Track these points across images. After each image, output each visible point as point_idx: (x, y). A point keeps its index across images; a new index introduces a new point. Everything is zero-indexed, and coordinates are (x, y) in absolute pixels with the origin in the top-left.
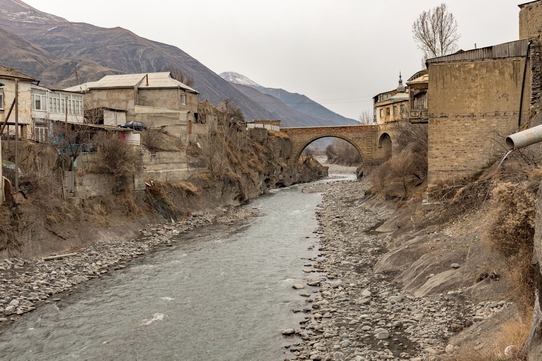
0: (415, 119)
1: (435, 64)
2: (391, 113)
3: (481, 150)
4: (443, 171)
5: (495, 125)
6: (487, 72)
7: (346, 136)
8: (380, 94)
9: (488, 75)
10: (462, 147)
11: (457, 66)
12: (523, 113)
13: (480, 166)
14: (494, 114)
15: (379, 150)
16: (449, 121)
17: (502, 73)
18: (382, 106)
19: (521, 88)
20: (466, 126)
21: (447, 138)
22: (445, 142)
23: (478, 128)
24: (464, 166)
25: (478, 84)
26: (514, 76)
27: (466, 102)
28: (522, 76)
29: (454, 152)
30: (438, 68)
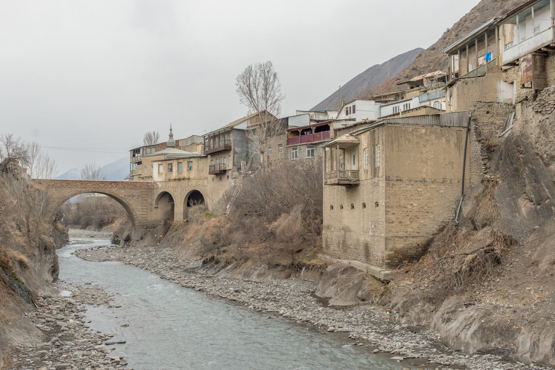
0: (344, 180)
1: (390, 125)
2: (175, 169)
3: (432, 216)
4: (399, 237)
5: (443, 191)
6: (436, 139)
7: (116, 192)
8: (143, 147)
9: (436, 142)
10: (415, 212)
11: (410, 129)
12: (465, 181)
13: (431, 233)
14: (442, 181)
15: (155, 210)
16: (403, 185)
17: (448, 141)
18: (161, 161)
19: (463, 158)
20: (418, 191)
21: (402, 202)
22: (400, 206)
23: (429, 194)
24: (417, 233)
25: (428, 150)
26: (458, 145)
27: (418, 167)
28: (464, 146)
29: (409, 217)
30: (393, 128)
